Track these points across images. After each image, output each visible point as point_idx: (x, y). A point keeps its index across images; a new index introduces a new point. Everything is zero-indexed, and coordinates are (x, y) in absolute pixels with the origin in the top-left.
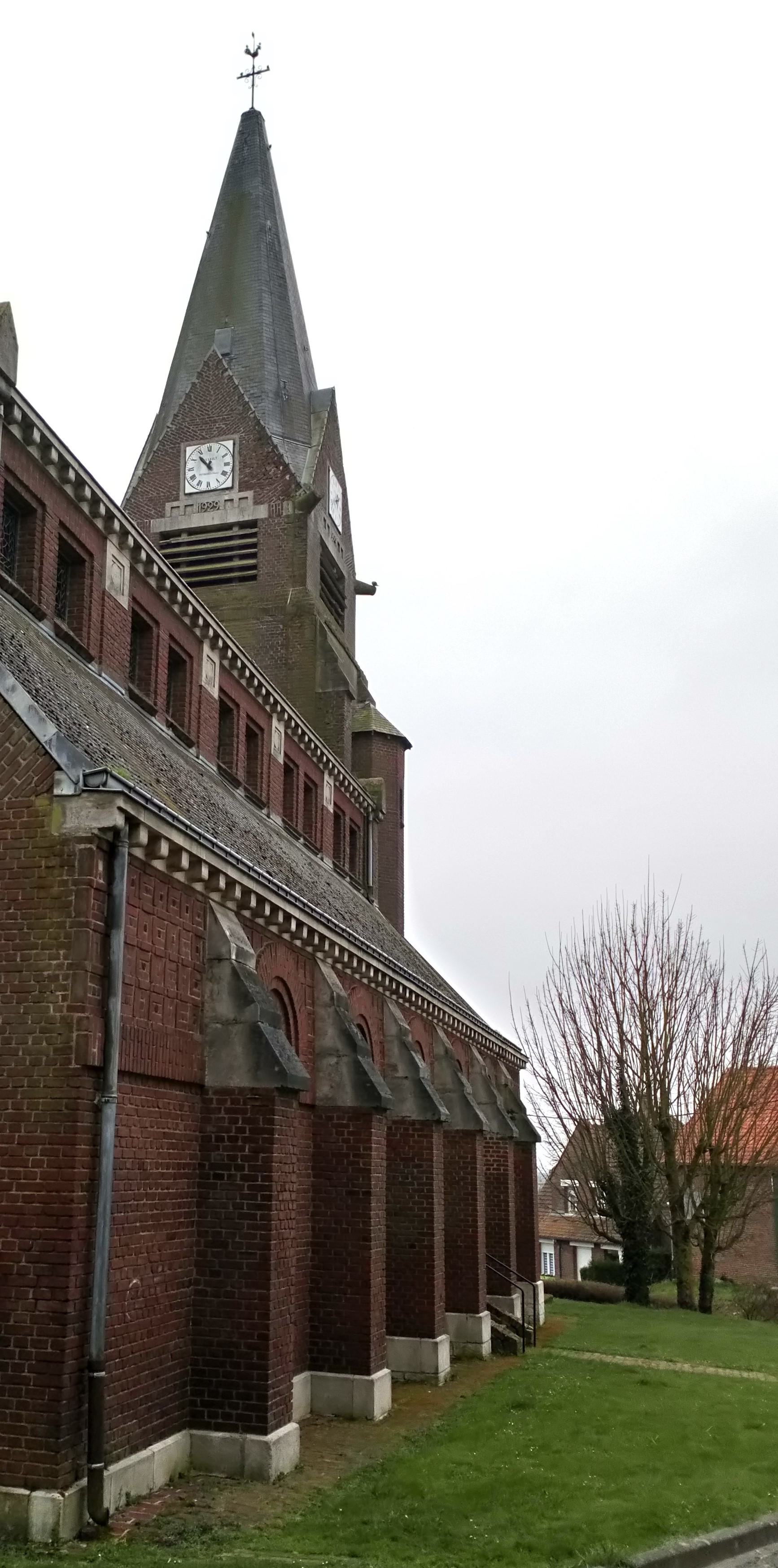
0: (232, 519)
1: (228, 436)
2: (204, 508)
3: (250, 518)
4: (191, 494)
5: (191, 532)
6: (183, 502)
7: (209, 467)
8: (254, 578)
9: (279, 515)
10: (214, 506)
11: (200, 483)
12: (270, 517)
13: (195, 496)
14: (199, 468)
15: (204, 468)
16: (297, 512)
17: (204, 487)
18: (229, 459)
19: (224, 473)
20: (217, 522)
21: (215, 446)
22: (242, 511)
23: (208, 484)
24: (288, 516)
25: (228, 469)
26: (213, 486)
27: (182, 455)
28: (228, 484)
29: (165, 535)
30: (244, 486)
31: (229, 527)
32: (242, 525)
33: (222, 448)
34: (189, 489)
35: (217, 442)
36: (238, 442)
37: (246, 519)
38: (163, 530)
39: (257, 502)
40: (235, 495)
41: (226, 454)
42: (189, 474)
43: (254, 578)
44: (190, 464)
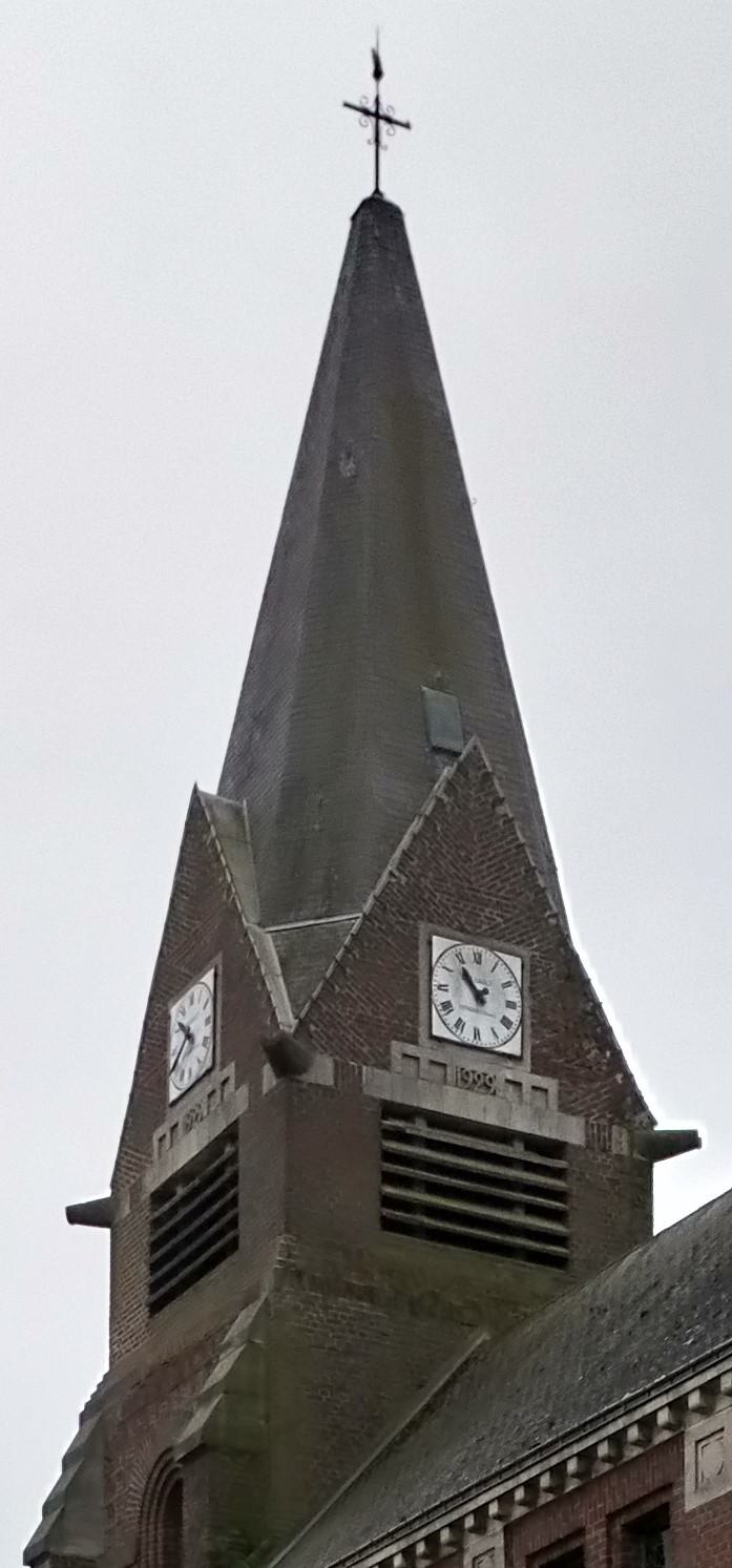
0: (521, 1124)
1: (516, 949)
3: (554, 1136)
5: (436, 1120)
6: (425, 1051)
7: (480, 997)
8: (560, 1262)
10: (486, 1085)
11: (460, 1023)
12: (589, 1146)
13: (450, 1049)
14: (458, 989)
15: (467, 997)
16: (636, 1155)
17: (467, 1036)
18: (513, 994)
19: (506, 1022)
20: (491, 1119)
21: (488, 957)
22: (538, 1114)
23: (477, 1033)
24: (619, 1157)
25: (514, 1016)
26: (486, 1040)
27: (422, 951)
28: (513, 1048)
29: (390, 1109)
32: (532, 1143)
33: (501, 968)
34: (438, 1030)
35: (492, 949)
36: (527, 961)
37: (546, 1133)
38: (387, 1097)
39: (565, 1108)
40: (529, 1079)
41: (508, 984)
42: (439, 997)
43: (560, 1262)
44: (440, 976)
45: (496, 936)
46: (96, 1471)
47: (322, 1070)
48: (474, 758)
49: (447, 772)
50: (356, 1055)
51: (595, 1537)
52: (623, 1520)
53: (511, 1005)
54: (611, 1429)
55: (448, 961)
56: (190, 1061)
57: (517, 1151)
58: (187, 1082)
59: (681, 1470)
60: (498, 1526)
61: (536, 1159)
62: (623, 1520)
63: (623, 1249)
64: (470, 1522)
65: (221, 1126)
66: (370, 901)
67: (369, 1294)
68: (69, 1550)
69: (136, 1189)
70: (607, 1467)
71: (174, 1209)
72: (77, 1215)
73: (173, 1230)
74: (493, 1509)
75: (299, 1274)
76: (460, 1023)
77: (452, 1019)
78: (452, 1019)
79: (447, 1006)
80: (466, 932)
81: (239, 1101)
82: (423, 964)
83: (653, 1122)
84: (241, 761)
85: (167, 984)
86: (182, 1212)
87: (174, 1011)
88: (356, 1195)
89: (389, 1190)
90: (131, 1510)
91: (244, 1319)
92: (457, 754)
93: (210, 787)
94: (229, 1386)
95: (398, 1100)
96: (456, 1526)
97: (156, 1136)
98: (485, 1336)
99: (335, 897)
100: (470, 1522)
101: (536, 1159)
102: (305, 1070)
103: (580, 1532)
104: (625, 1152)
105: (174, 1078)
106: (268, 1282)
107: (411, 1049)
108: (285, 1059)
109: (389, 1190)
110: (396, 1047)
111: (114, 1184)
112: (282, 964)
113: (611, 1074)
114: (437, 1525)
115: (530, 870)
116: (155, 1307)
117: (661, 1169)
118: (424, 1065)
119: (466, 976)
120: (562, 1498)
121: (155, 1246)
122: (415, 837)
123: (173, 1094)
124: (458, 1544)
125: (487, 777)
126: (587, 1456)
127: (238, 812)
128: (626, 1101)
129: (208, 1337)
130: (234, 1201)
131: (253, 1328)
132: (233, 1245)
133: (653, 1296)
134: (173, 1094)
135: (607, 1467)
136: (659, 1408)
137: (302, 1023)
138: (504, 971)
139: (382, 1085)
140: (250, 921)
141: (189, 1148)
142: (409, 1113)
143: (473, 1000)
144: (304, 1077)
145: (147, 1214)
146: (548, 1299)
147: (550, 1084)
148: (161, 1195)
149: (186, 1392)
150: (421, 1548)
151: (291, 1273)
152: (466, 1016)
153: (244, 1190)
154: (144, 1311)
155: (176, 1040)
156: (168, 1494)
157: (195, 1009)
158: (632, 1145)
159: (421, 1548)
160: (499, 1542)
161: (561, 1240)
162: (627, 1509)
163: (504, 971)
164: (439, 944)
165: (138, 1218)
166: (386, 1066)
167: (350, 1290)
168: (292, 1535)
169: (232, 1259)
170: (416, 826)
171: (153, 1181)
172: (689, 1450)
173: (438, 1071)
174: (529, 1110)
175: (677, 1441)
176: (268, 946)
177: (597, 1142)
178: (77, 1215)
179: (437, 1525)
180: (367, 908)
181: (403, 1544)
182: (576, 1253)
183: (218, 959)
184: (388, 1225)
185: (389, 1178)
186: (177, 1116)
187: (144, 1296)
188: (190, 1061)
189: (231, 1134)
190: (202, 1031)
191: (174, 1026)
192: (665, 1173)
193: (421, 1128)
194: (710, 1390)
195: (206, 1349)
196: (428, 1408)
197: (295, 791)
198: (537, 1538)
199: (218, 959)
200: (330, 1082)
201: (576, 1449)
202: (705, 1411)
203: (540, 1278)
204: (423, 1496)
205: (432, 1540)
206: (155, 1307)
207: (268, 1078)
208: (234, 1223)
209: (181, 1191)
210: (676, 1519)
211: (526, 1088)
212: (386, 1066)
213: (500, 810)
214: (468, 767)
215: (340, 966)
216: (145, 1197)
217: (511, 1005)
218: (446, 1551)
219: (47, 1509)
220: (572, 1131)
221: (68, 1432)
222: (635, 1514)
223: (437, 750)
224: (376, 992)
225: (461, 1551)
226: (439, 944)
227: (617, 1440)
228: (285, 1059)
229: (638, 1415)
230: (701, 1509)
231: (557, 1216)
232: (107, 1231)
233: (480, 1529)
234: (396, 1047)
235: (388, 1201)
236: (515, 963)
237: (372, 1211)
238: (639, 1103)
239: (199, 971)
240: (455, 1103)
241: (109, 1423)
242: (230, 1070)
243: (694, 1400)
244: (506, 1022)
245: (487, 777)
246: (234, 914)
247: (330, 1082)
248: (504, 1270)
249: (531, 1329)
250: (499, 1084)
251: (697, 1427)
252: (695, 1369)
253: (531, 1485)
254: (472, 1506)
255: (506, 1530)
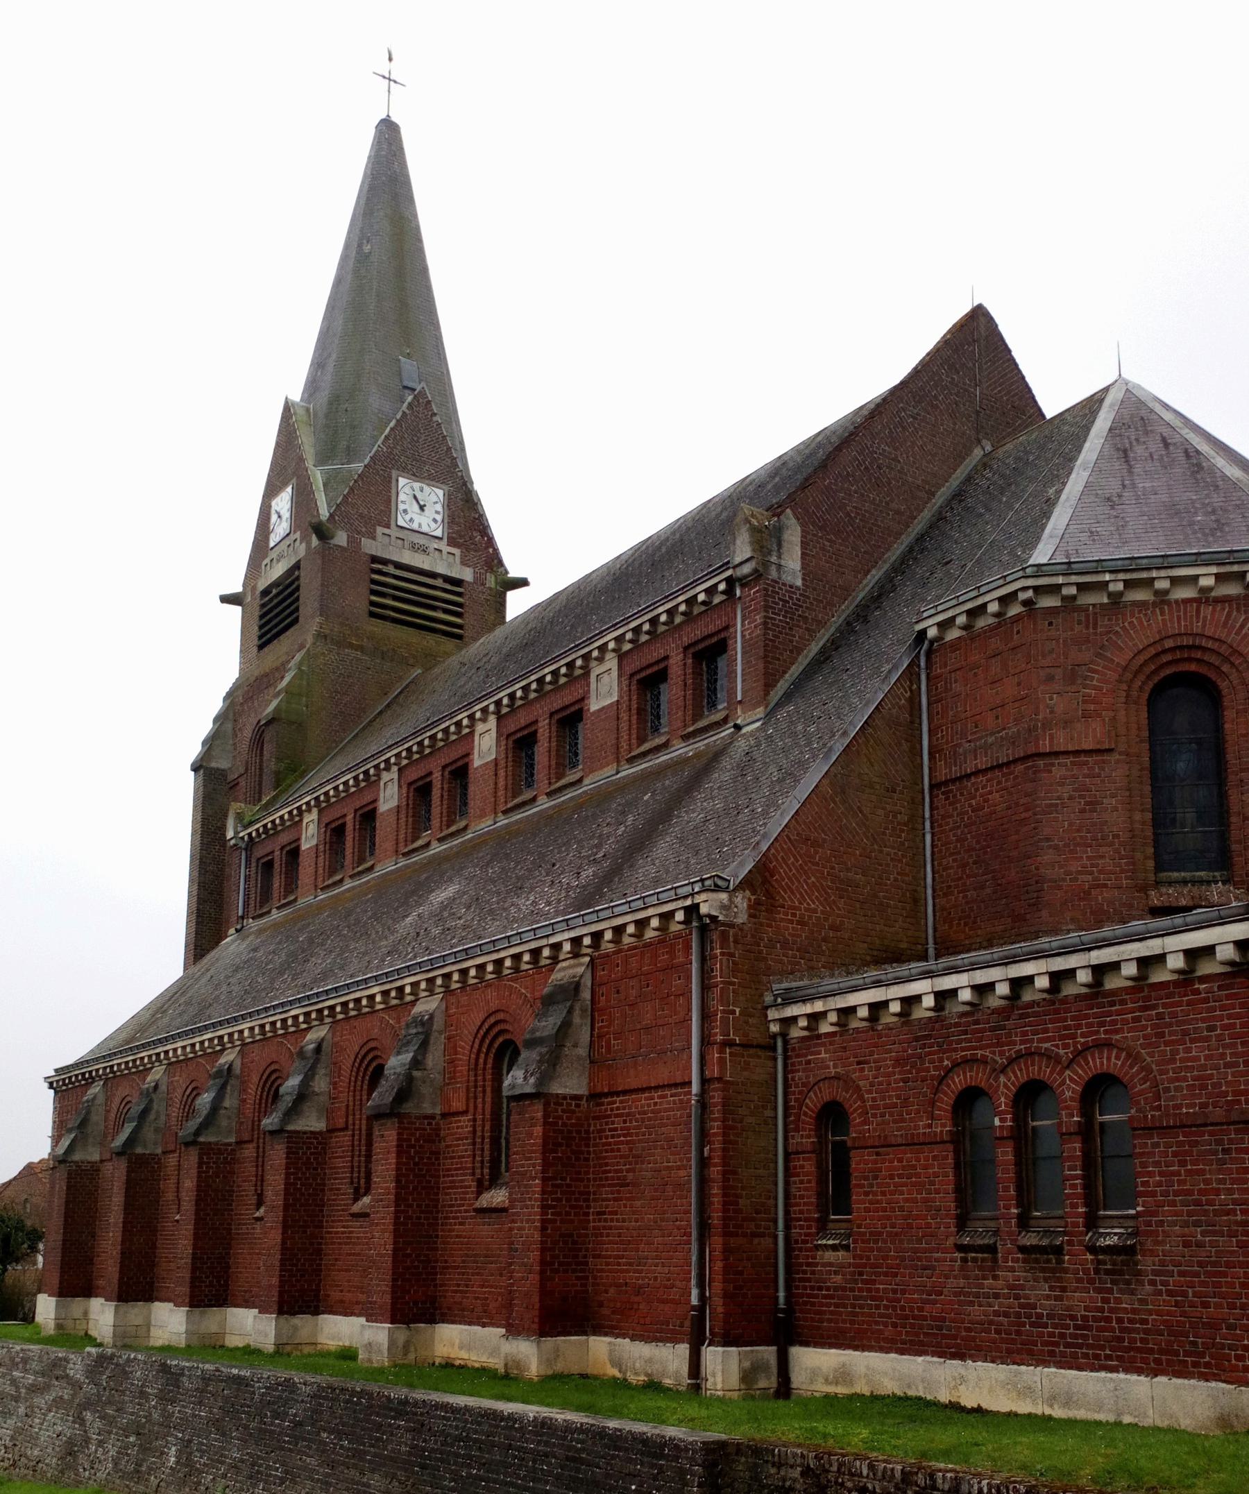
0: (441, 569)
2: (415, 548)
3: (458, 576)
4: (402, 527)
5: (398, 566)
6: (393, 532)
7: (422, 508)
8: (460, 637)
9: (483, 584)
10: (424, 550)
11: (411, 520)
17: (415, 526)
18: (439, 507)
19: (435, 521)
20: (426, 567)
21: (427, 489)
22: (450, 565)
23: (420, 525)
24: (490, 589)
25: (439, 518)
26: (425, 529)
28: (438, 533)
29: (375, 559)
30: (452, 542)
31: (433, 575)
32: (447, 579)
34: (401, 522)
37: (453, 575)
39: (464, 563)
40: (446, 549)
42: (401, 507)
43: (460, 637)
44: (402, 497)
45: (432, 479)
46: (229, 726)
47: (341, 538)
48: (422, 394)
49: (410, 398)
50: (359, 533)
51: (437, 775)
52: (449, 769)
53: (437, 512)
54: (443, 726)
55: (407, 489)
56: (280, 528)
57: (439, 582)
58: (278, 539)
59: (473, 748)
60: (395, 768)
61: (448, 587)
62: (449, 769)
63: (491, 629)
64: (382, 766)
65: (293, 562)
66: (368, 458)
67: (361, 648)
68: (213, 765)
69: (254, 588)
70: (442, 744)
71: (271, 600)
72: (226, 599)
73: (272, 611)
74: (393, 760)
75: (325, 637)
76: (411, 520)
77: (407, 518)
78: (407, 518)
79: (405, 511)
80: (416, 476)
81: (302, 550)
82: (393, 491)
83: (507, 572)
84: (312, 385)
85: (272, 490)
86: (275, 601)
87: (273, 503)
88: (357, 599)
89: (373, 598)
90: (244, 747)
91: (298, 657)
92: (414, 390)
93: (296, 397)
94: (287, 690)
95: (379, 554)
96: (376, 767)
97: (264, 563)
98: (420, 671)
99: (351, 454)
100: (382, 766)
101: (448, 587)
102: (332, 538)
103: (430, 774)
104: (493, 586)
105: (272, 536)
106: (310, 640)
107: (386, 531)
108: (321, 531)
109: (373, 598)
110: (380, 530)
111: (244, 585)
112: (324, 485)
113: (487, 548)
114: (368, 766)
115: (449, 449)
116: (261, 647)
117: (512, 596)
118: (393, 538)
119: (415, 497)
120: (423, 757)
121: (261, 617)
122: (392, 429)
123: (272, 544)
124: (378, 775)
125: (429, 402)
126: (433, 737)
127: (308, 410)
128: (493, 561)
129: (283, 664)
130: (297, 599)
131: (301, 663)
132: (296, 621)
133: (485, 660)
134: (272, 544)
135: (442, 744)
136: (463, 716)
137: (331, 515)
138: (435, 496)
139: (370, 547)
140: (310, 463)
141: (278, 571)
142: (385, 562)
143: (419, 508)
144: (332, 542)
145: (258, 602)
146: (448, 655)
147: (457, 551)
148: (265, 592)
149: (271, 691)
150: (361, 777)
151: (321, 636)
152: (415, 517)
153: (303, 593)
154: (255, 649)
155: (274, 517)
156: (258, 741)
157: (283, 503)
158: (496, 583)
159: (361, 777)
160: (396, 776)
161: (460, 627)
162: (451, 764)
163: (435, 496)
164: (402, 481)
165: (254, 601)
166: (374, 538)
167: (351, 646)
168: (318, 764)
169: (296, 627)
170: (392, 424)
171: (262, 584)
172: (477, 738)
173: (400, 542)
174: (446, 562)
175: (472, 733)
176: (317, 477)
177: (480, 581)
178: (226, 599)
179: (368, 766)
180: (366, 461)
181: (353, 774)
182: (467, 633)
183: (294, 480)
184: (372, 615)
185: (373, 592)
186: (273, 555)
187: (256, 642)
188: (280, 528)
189: (297, 566)
190: (286, 515)
191: (273, 511)
192: (512, 596)
193: (391, 569)
194: (485, 710)
195: (281, 669)
196: (388, 706)
197: (335, 400)
198: (413, 774)
199: (294, 480)
200: (345, 544)
201: (428, 734)
202: (484, 720)
203: (449, 644)
204: (374, 749)
205: (366, 773)
206: (261, 647)
207: (315, 541)
208: (297, 609)
209: (274, 591)
210: (471, 771)
211: (444, 552)
212: (374, 538)
213: (435, 419)
214: (419, 396)
215: (352, 489)
216: (258, 593)
217: (437, 512)
218: (374, 778)
219: (204, 743)
220: (467, 575)
221: (216, 705)
222: (454, 767)
223: (406, 387)
224: (369, 501)
225: (379, 779)
226: (402, 481)
227: (446, 731)
228: (321, 531)
229: (455, 720)
230: (481, 766)
231: (459, 615)
232: (239, 609)
233: (387, 769)
234: (380, 530)
235: (372, 604)
236: (440, 493)
237: (363, 607)
238: (501, 563)
239: (285, 485)
240: (408, 558)
241: (239, 701)
242: (298, 535)
243: (478, 715)
244: (435, 521)
245: (429, 402)
246: (301, 460)
247: (345, 544)
248: (430, 640)
249: (437, 670)
250: (431, 550)
251: (480, 727)
252: (479, 700)
253: (409, 750)
254: (383, 758)
255: (399, 770)
